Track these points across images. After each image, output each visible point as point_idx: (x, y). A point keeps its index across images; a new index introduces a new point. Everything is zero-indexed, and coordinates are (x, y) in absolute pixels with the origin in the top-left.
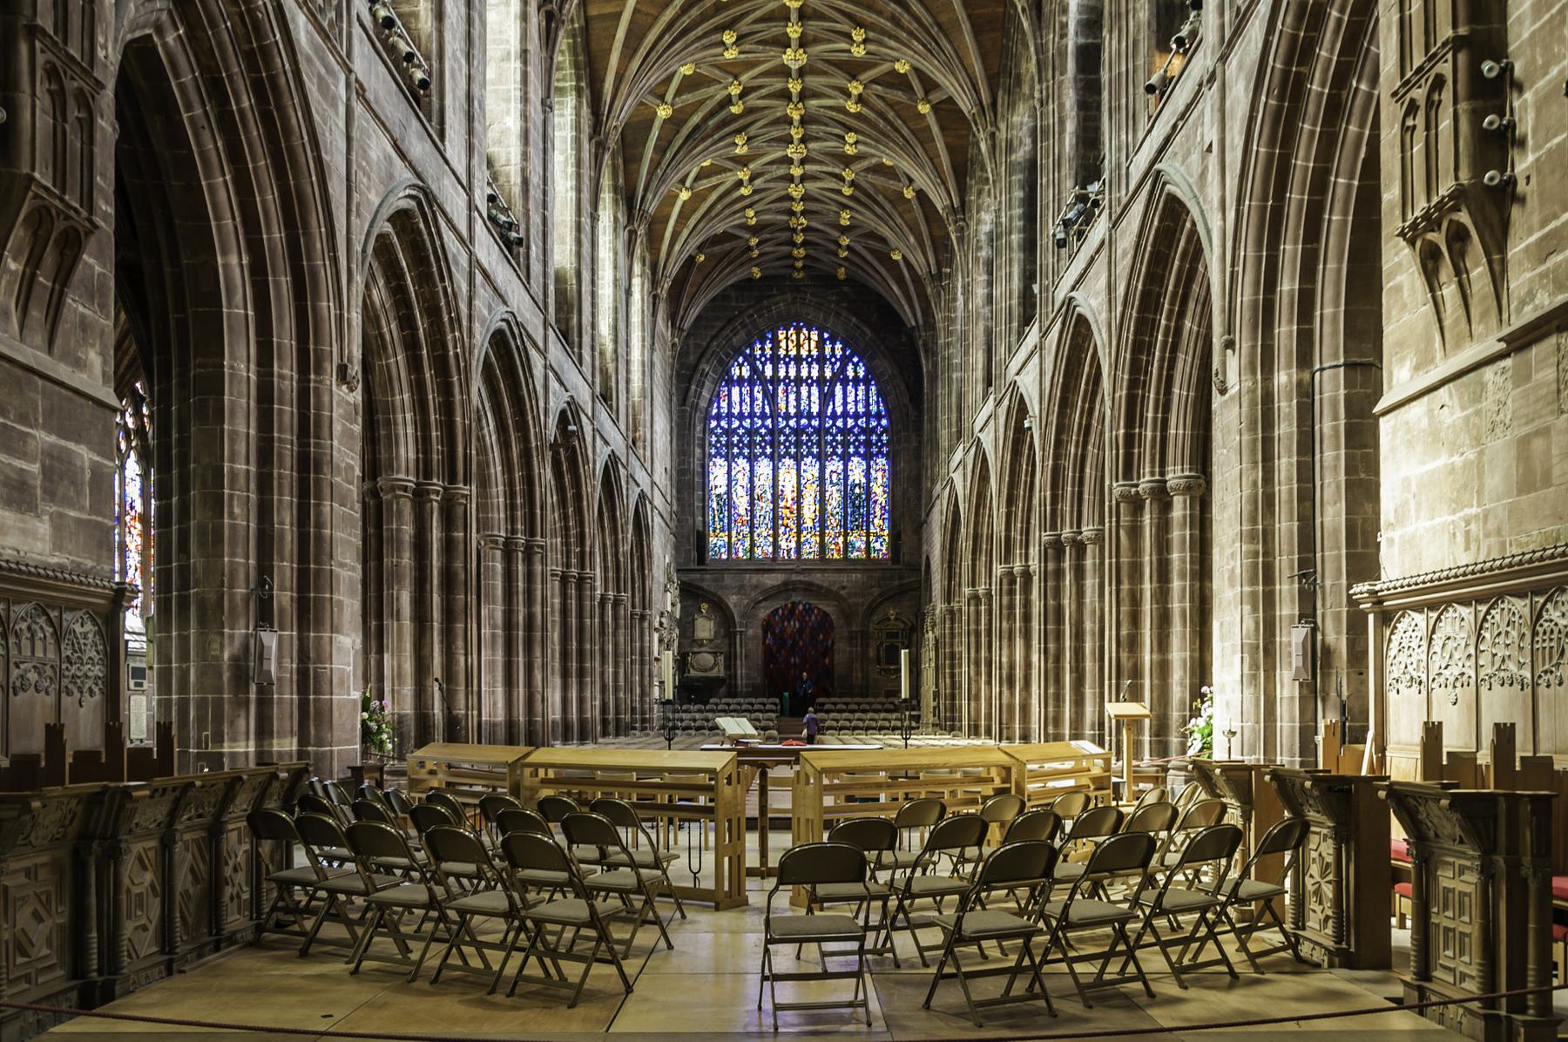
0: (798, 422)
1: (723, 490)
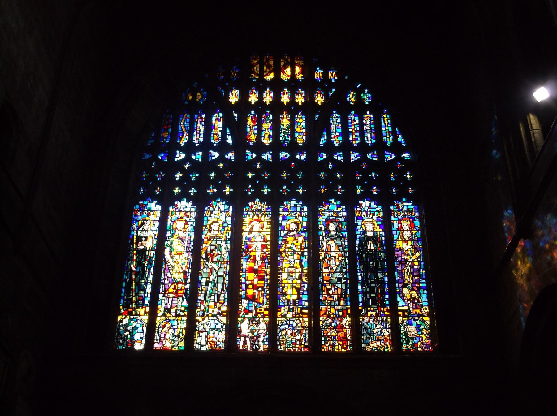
0: (275, 156)
1: (150, 244)
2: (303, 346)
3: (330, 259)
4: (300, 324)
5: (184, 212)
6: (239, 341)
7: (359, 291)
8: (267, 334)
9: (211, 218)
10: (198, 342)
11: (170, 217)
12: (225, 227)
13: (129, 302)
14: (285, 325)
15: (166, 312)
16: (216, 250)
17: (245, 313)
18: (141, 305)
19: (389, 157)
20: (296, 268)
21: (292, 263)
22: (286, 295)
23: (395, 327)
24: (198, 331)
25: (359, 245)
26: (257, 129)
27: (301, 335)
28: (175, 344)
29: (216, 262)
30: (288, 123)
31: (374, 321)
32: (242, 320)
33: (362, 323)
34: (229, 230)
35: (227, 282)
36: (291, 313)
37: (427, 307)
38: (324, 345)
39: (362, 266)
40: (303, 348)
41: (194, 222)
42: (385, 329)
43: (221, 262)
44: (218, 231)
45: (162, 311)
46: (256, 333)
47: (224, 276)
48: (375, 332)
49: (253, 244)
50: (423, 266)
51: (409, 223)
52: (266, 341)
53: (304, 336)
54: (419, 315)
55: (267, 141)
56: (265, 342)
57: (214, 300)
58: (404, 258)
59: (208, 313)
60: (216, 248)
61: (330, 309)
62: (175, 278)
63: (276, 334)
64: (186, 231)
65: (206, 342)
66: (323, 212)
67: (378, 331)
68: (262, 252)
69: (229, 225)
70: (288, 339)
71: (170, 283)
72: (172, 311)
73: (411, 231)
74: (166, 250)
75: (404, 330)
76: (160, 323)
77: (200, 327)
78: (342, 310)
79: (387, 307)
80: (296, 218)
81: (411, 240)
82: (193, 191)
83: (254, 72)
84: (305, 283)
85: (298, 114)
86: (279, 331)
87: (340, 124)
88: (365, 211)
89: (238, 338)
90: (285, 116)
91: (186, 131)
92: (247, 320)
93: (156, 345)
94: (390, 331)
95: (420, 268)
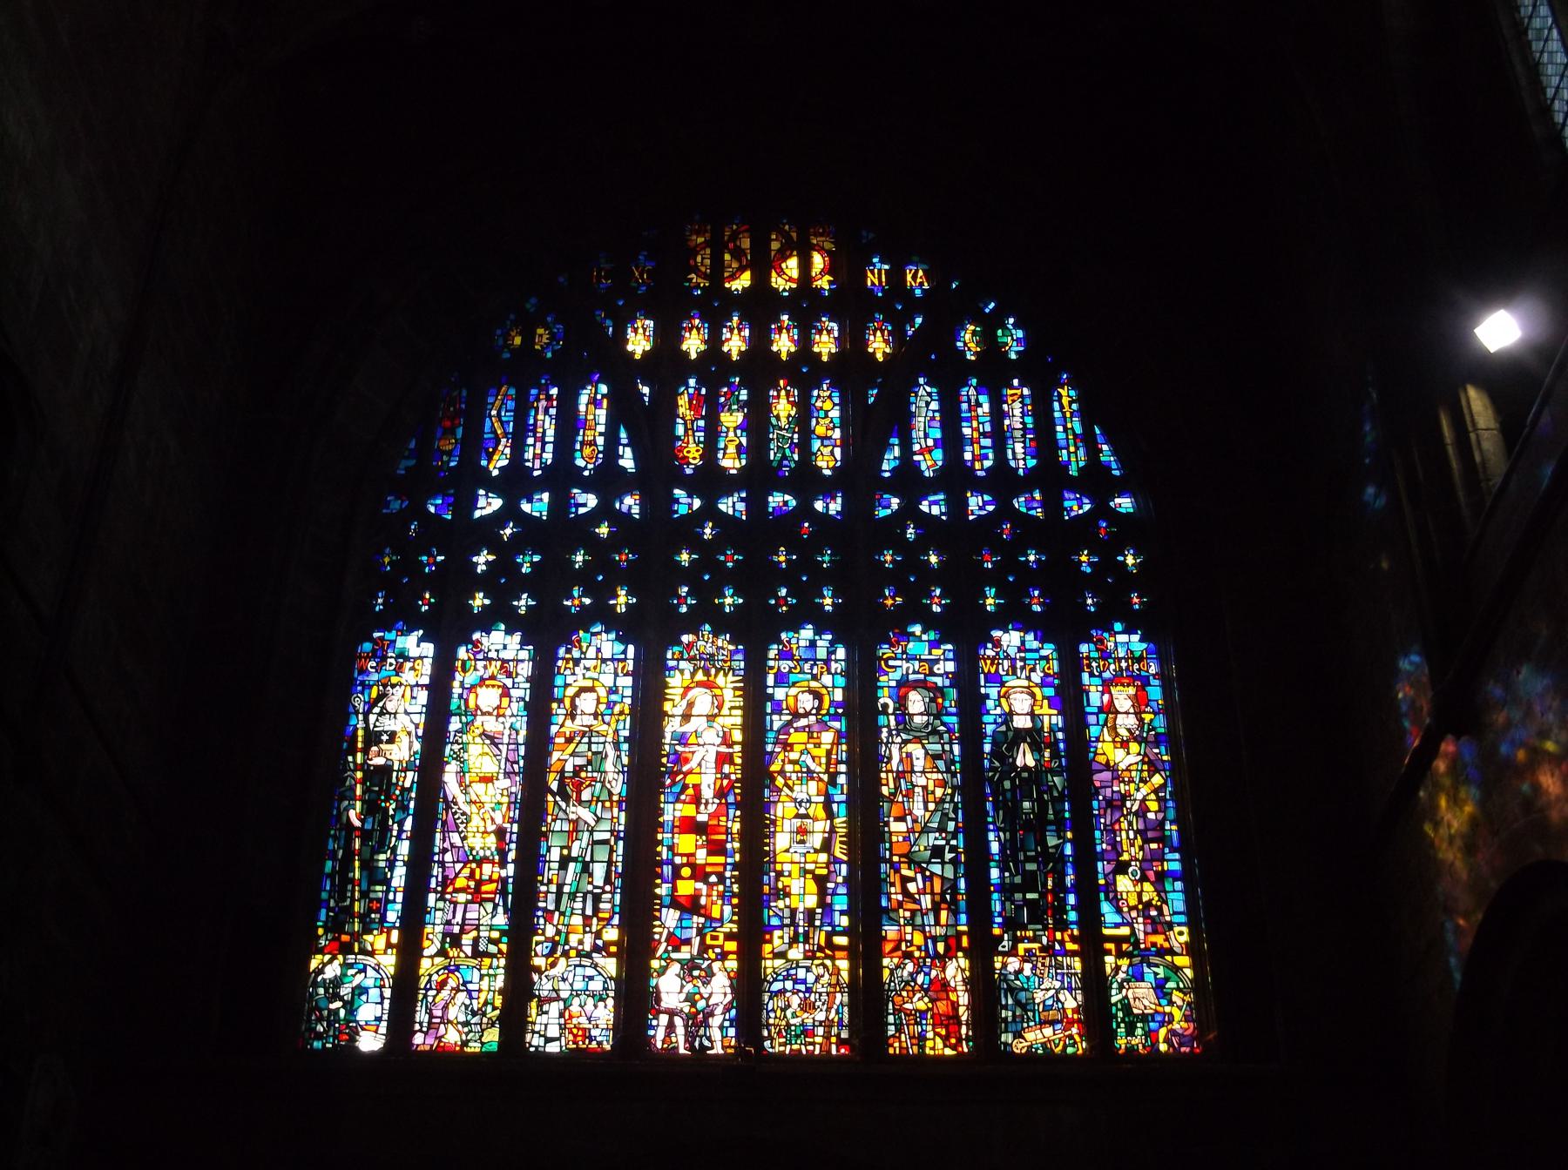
0: (756, 503)
1: (401, 752)
2: (834, 1040)
3: (909, 794)
5: (499, 663)
6: (653, 1027)
7: (994, 885)
8: (733, 1007)
9: (574, 678)
10: (537, 1028)
11: (458, 677)
12: (615, 703)
13: (342, 916)
14: (783, 980)
15: (447, 946)
16: (590, 768)
17: (670, 948)
18: (376, 926)
19: (1075, 508)
20: (815, 819)
21: (803, 804)
22: (788, 895)
23: (1095, 984)
25: (992, 753)
26: (705, 430)
27: (829, 1010)
28: (472, 1034)
30: (793, 413)
31: (1034, 967)
32: (661, 967)
33: (1000, 974)
34: (627, 711)
35: (620, 859)
36: (801, 945)
37: (1185, 929)
38: (893, 1036)
39: (1001, 812)
40: (834, 1048)
41: (528, 691)
42: (1066, 991)
43: (603, 802)
44: (595, 715)
45: (435, 940)
46: (701, 1004)
47: (612, 843)
48: (1037, 1001)
49: (693, 753)
50: (1171, 814)
51: (1132, 691)
52: (731, 1026)
53: (837, 1012)
54: (1162, 952)
55: (731, 462)
56: (727, 1028)
57: (584, 909)
58: (1119, 791)
59: (567, 947)
60: (589, 762)
61: (912, 934)
62: (472, 849)
63: (760, 1006)
64: (504, 716)
66: (891, 663)
67: (1047, 997)
68: (719, 776)
69: (625, 700)
70: (792, 1021)
71: (458, 862)
72: (463, 942)
73: (1138, 714)
74: (448, 768)
75: (1120, 992)
76: (430, 975)
77: (544, 987)
78: (946, 938)
79: (1072, 930)
80: (815, 678)
81: (1139, 740)
82: (523, 603)
83: (696, 270)
84: (841, 862)
85: (819, 388)
86: (766, 997)
87: (937, 414)
88: (1007, 657)
89: (650, 1017)
90: (783, 393)
91: (506, 434)
93: (418, 1039)
94: (1079, 998)
95: (1164, 819)
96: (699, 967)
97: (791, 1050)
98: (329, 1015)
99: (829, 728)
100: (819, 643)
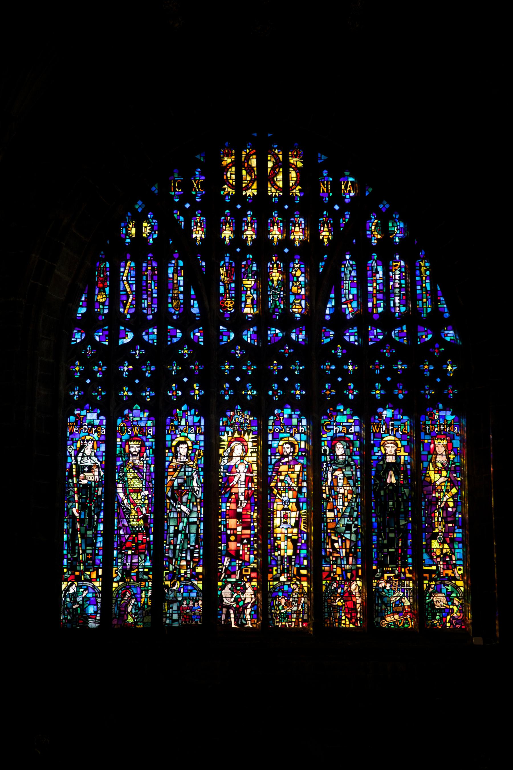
2: (300, 620)
3: (336, 498)
4: (297, 589)
12: (196, 450)
18: (91, 567)
20: (292, 511)
22: (280, 549)
24: (168, 600)
27: (298, 606)
29: (187, 502)
35: (202, 531)
36: (286, 574)
38: (327, 618)
39: (379, 507)
40: (300, 623)
41: (154, 443)
43: (193, 503)
45: (119, 573)
46: (241, 604)
49: (234, 476)
53: (302, 607)
57: (186, 557)
60: (185, 481)
61: (336, 568)
64: (143, 457)
65: (178, 615)
66: (329, 427)
70: (282, 611)
71: (127, 534)
72: (132, 574)
76: (118, 591)
78: (351, 571)
80: (292, 436)
92: (229, 586)
96: (239, 585)
97: (282, 625)
98: (73, 611)
99: (297, 463)
100: (294, 416)
